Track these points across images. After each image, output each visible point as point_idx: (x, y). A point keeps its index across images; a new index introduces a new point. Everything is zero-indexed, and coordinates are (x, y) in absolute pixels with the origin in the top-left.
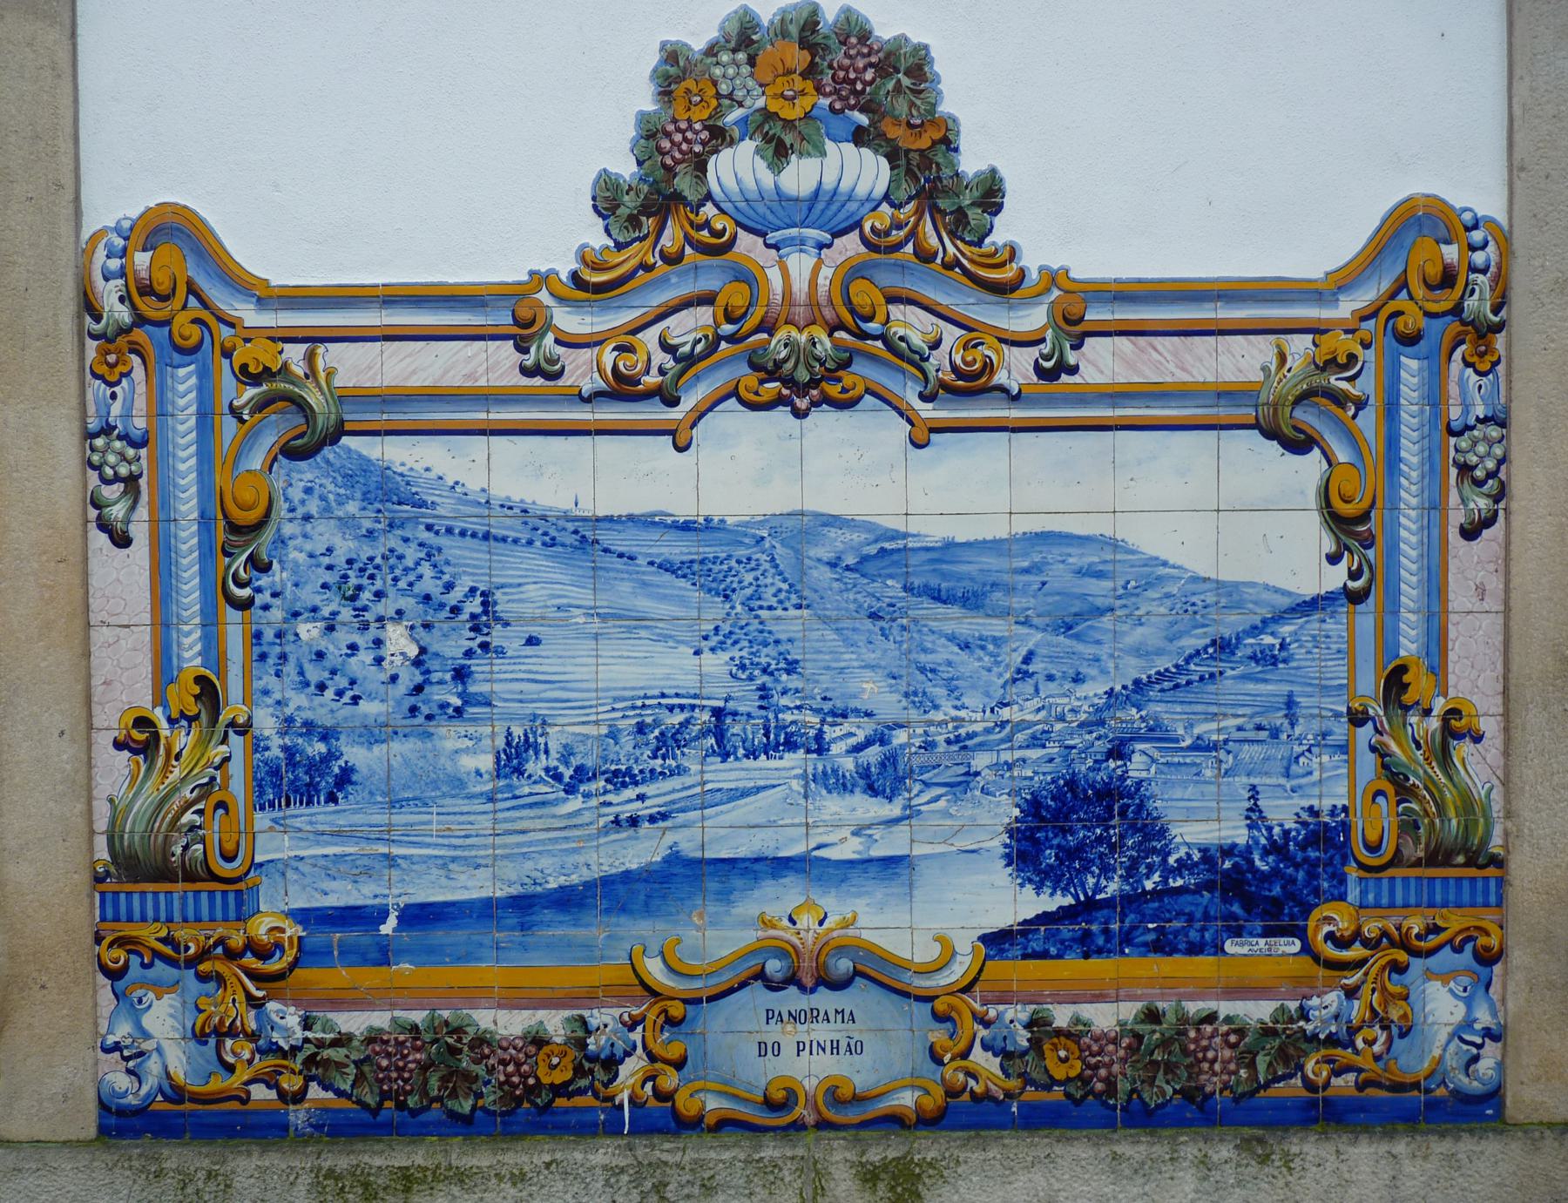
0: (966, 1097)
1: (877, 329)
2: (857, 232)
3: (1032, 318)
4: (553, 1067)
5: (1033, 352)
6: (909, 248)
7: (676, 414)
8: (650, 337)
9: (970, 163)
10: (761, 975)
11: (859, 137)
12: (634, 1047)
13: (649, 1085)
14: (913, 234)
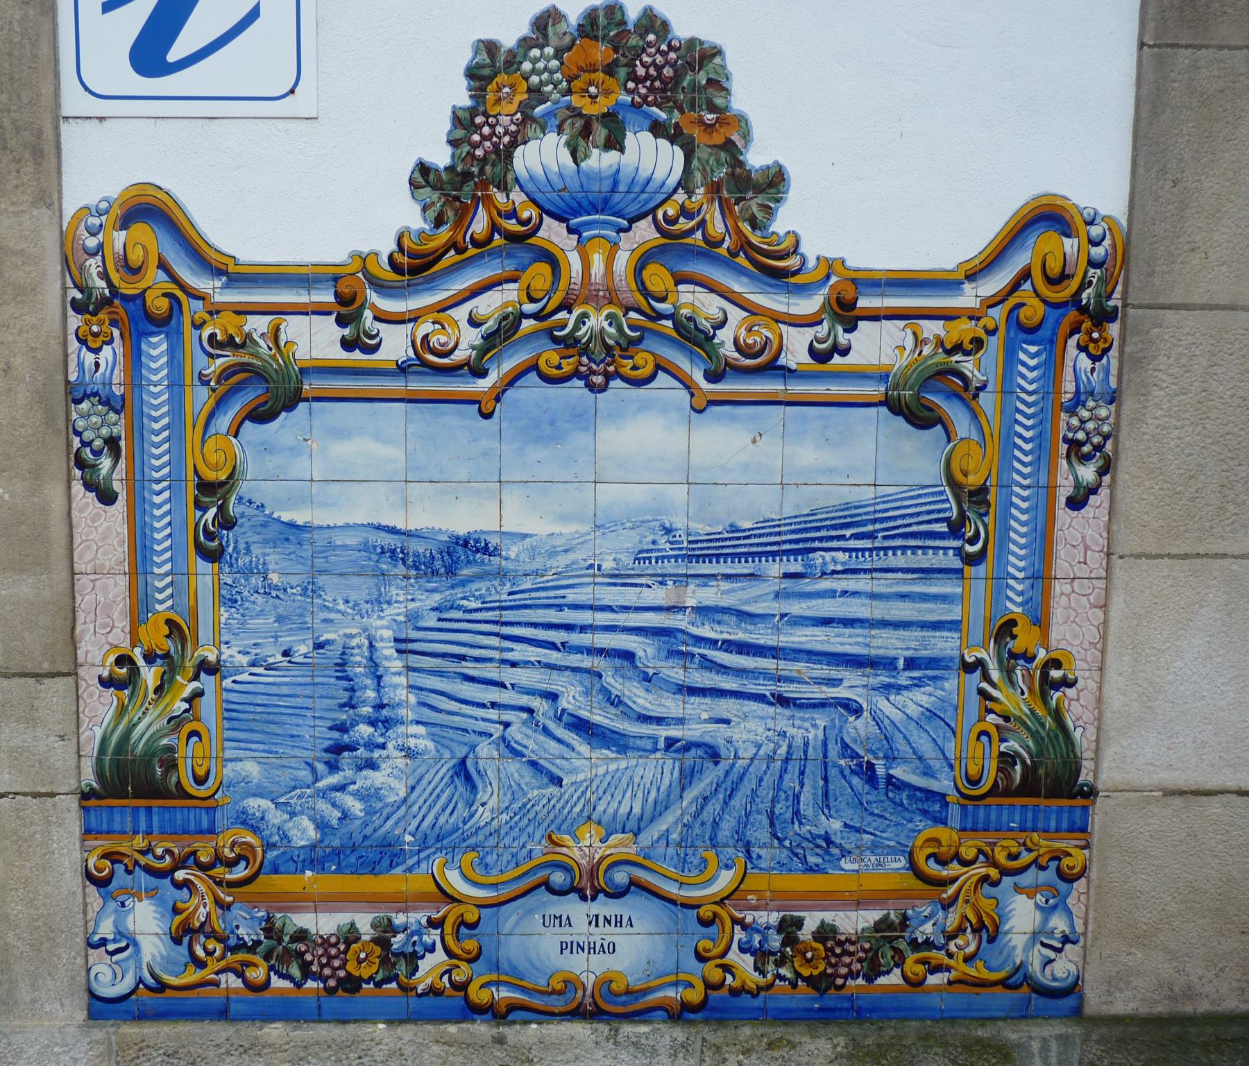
0: (724, 992)
1: (666, 309)
2: (650, 218)
3: (809, 305)
4: (360, 962)
5: (808, 334)
6: (699, 235)
7: (484, 384)
8: (461, 313)
9: (756, 158)
10: (546, 885)
11: (657, 129)
12: (434, 944)
13: (446, 978)
14: (702, 224)
